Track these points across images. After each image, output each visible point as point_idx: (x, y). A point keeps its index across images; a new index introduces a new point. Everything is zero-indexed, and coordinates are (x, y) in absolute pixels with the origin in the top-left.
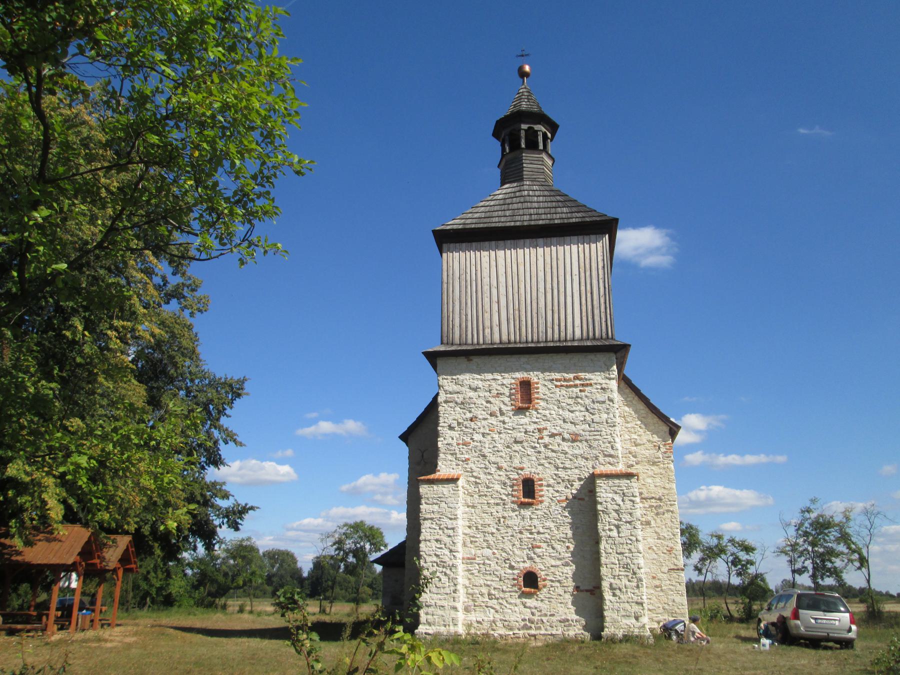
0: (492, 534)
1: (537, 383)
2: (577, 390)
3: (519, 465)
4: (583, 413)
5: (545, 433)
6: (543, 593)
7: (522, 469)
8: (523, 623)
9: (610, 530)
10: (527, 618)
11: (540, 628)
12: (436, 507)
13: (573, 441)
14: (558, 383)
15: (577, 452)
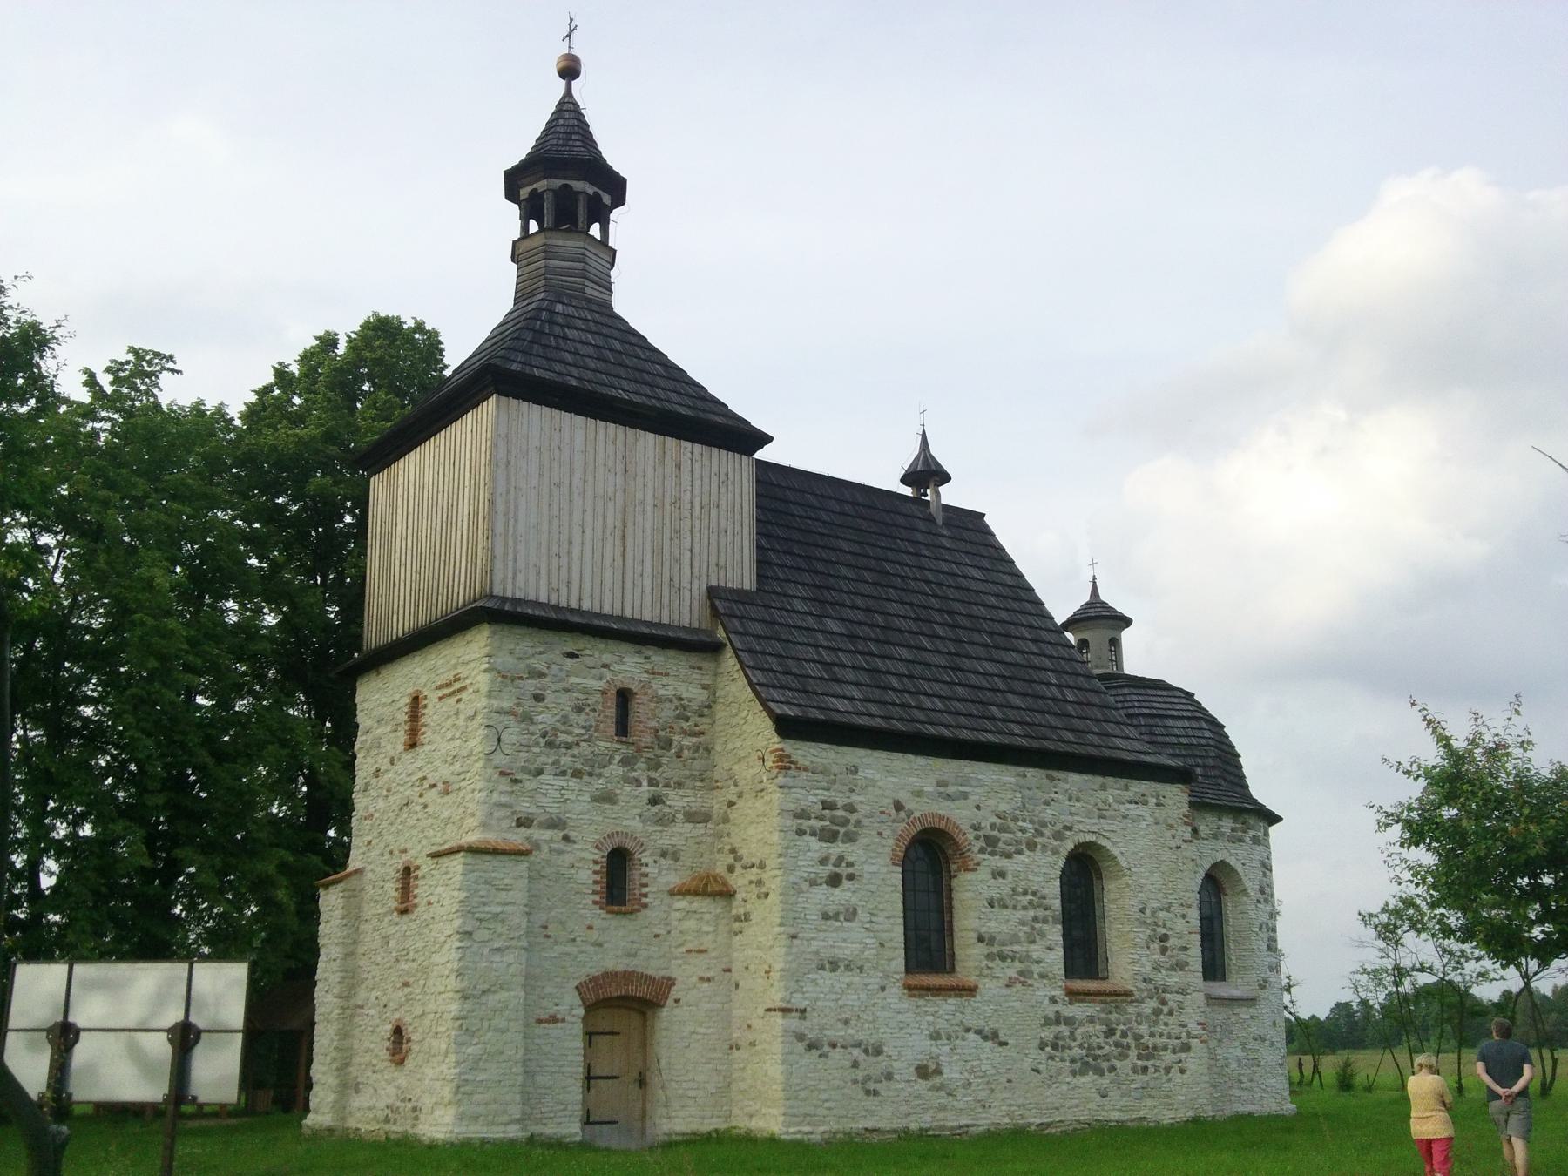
2: (454, 699)
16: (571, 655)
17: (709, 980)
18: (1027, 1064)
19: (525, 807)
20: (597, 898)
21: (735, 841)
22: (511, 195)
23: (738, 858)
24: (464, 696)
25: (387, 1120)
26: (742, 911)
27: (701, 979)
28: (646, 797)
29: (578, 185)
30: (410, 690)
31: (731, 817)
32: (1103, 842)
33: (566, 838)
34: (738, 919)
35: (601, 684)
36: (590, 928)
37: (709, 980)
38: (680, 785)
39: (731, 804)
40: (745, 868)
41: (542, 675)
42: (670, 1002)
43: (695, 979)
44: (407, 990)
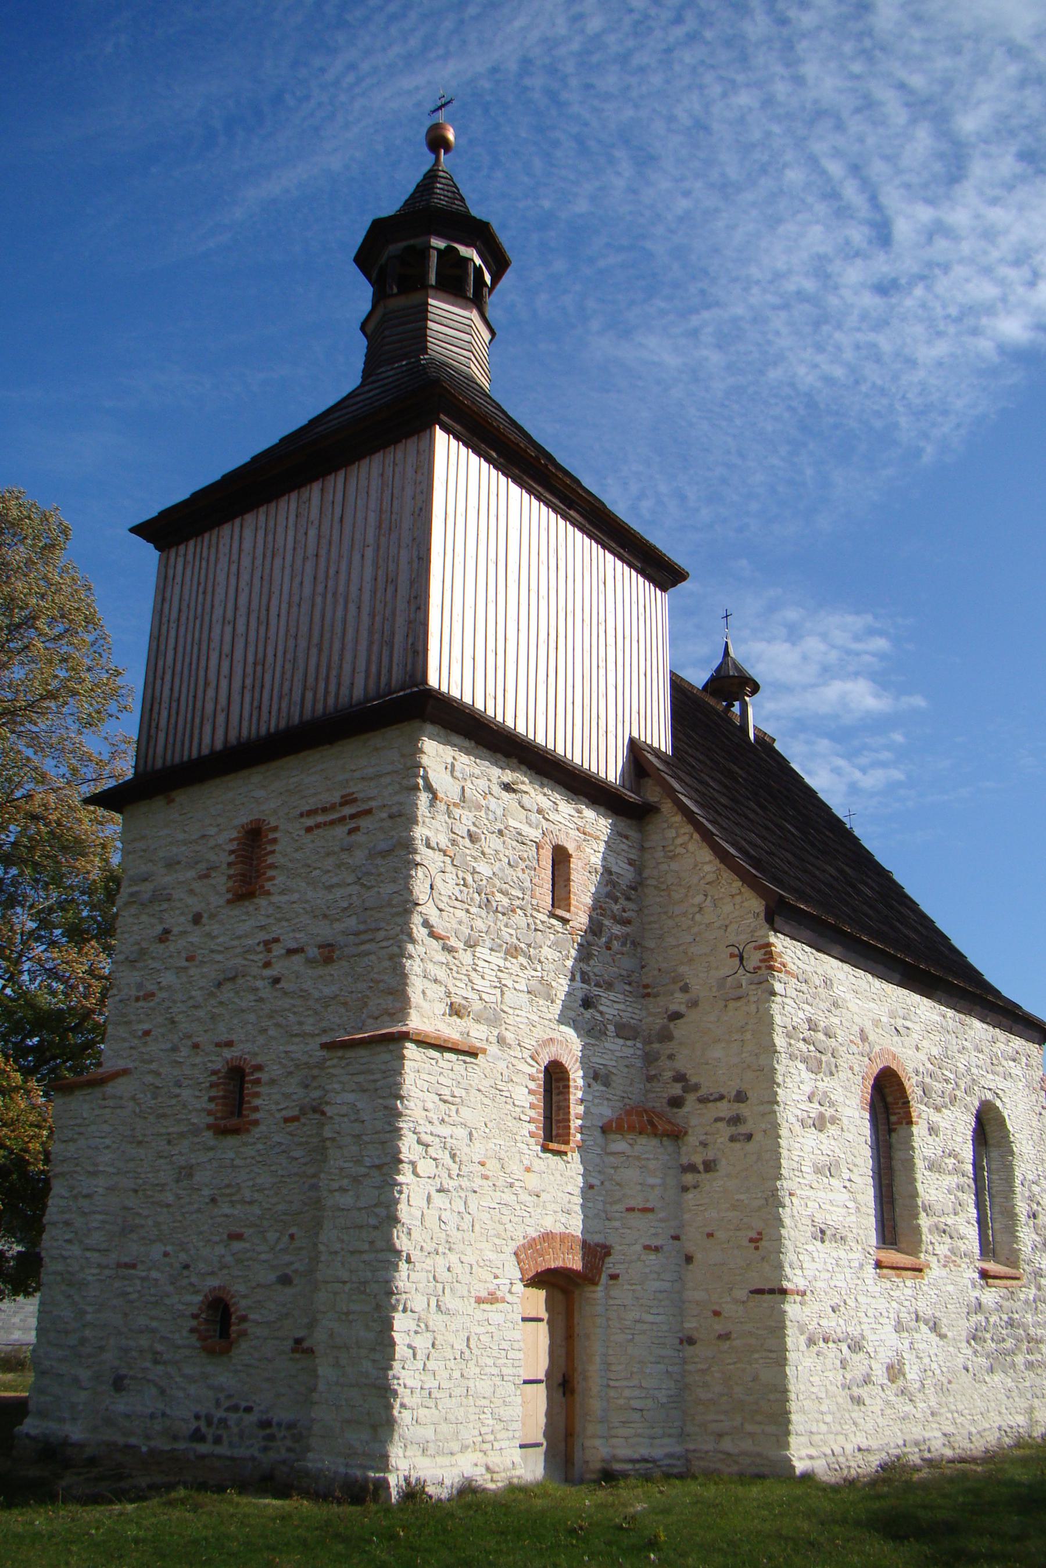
0: (168, 1206)
1: (275, 829)
2: (340, 831)
3: (225, 1037)
4: (350, 890)
5: (278, 950)
6: (242, 1352)
7: (229, 1044)
8: (194, 1425)
9: (342, 1190)
10: (203, 1413)
11: (218, 1440)
12: (72, 1147)
13: (328, 960)
14: (310, 822)
15: (327, 991)
16: (507, 787)
17: (657, 1249)
18: (960, 1361)
19: (461, 991)
20: (532, 1127)
21: (682, 1064)
22: (364, 259)
23: (691, 1088)
24: (364, 823)
25: (197, 1436)
26: (698, 1159)
27: (647, 1248)
28: (580, 995)
29: (464, 251)
30: (244, 819)
31: (677, 1033)
32: (998, 1103)
33: (501, 1040)
34: (691, 1168)
35: (535, 834)
36: (528, 1170)
37: (657, 1249)
38: (609, 986)
39: (676, 1016)
40: (703, 1100)
41: (479, 807)
42: (604, 1278)
43: (638, 1248)
44: (237, 1246)
